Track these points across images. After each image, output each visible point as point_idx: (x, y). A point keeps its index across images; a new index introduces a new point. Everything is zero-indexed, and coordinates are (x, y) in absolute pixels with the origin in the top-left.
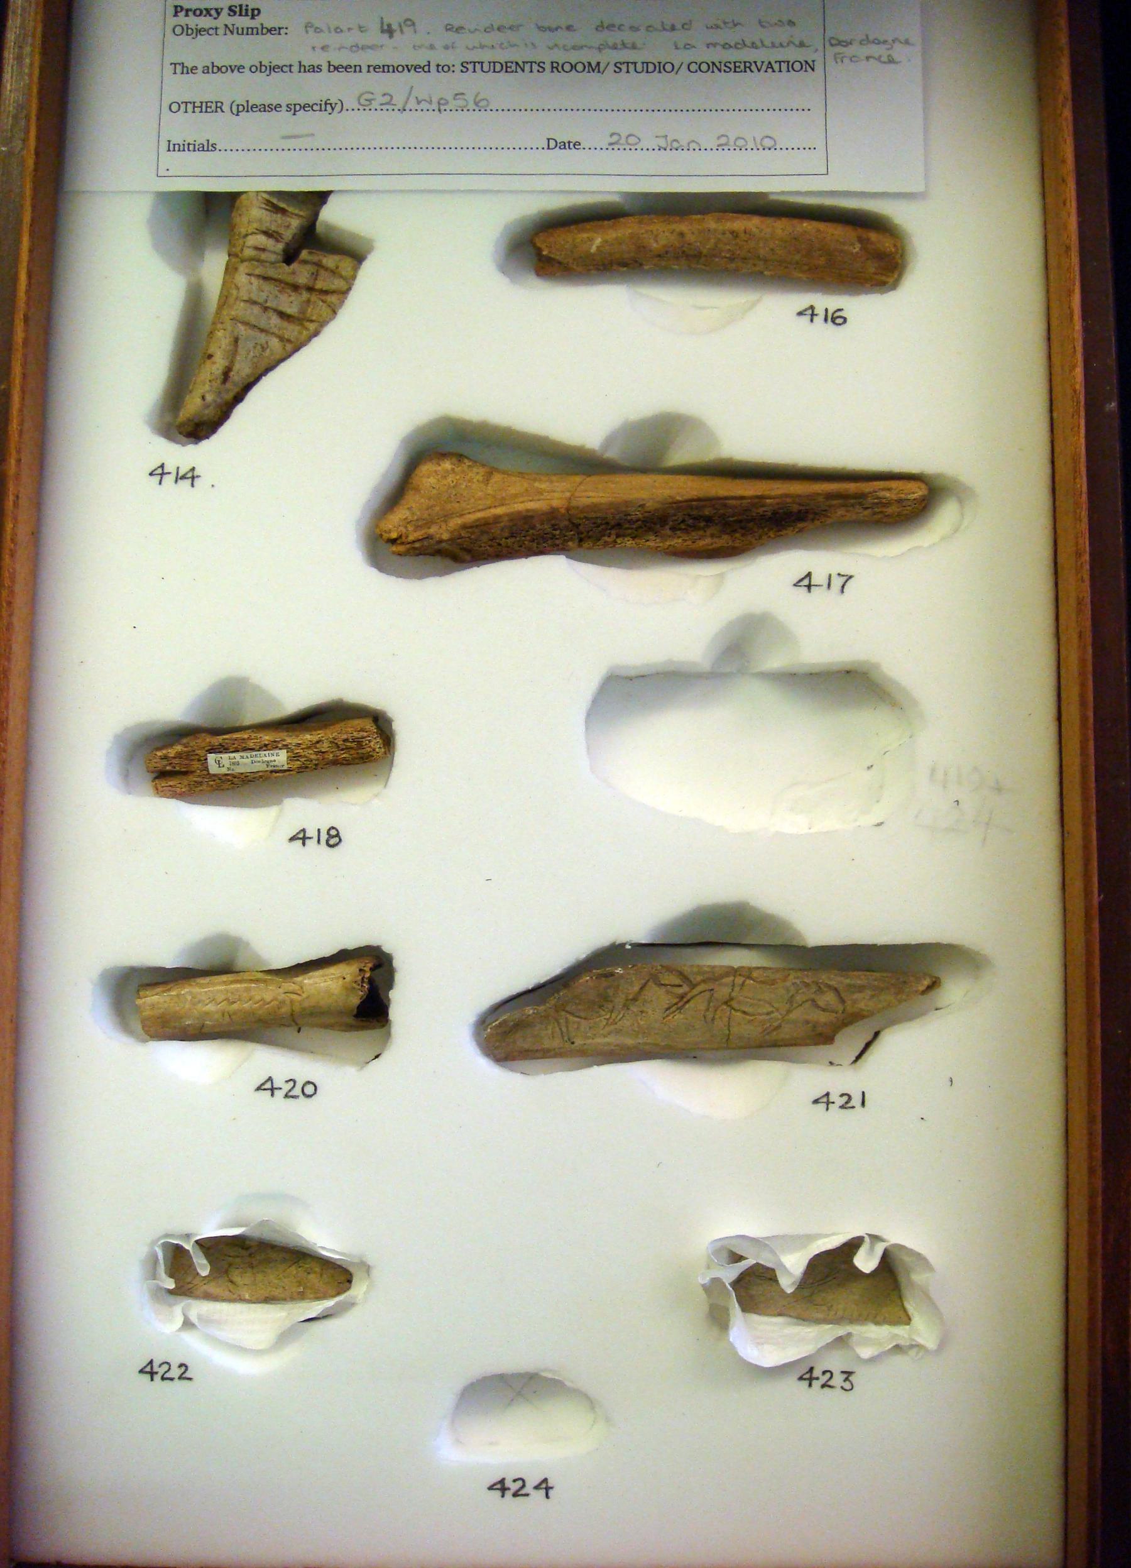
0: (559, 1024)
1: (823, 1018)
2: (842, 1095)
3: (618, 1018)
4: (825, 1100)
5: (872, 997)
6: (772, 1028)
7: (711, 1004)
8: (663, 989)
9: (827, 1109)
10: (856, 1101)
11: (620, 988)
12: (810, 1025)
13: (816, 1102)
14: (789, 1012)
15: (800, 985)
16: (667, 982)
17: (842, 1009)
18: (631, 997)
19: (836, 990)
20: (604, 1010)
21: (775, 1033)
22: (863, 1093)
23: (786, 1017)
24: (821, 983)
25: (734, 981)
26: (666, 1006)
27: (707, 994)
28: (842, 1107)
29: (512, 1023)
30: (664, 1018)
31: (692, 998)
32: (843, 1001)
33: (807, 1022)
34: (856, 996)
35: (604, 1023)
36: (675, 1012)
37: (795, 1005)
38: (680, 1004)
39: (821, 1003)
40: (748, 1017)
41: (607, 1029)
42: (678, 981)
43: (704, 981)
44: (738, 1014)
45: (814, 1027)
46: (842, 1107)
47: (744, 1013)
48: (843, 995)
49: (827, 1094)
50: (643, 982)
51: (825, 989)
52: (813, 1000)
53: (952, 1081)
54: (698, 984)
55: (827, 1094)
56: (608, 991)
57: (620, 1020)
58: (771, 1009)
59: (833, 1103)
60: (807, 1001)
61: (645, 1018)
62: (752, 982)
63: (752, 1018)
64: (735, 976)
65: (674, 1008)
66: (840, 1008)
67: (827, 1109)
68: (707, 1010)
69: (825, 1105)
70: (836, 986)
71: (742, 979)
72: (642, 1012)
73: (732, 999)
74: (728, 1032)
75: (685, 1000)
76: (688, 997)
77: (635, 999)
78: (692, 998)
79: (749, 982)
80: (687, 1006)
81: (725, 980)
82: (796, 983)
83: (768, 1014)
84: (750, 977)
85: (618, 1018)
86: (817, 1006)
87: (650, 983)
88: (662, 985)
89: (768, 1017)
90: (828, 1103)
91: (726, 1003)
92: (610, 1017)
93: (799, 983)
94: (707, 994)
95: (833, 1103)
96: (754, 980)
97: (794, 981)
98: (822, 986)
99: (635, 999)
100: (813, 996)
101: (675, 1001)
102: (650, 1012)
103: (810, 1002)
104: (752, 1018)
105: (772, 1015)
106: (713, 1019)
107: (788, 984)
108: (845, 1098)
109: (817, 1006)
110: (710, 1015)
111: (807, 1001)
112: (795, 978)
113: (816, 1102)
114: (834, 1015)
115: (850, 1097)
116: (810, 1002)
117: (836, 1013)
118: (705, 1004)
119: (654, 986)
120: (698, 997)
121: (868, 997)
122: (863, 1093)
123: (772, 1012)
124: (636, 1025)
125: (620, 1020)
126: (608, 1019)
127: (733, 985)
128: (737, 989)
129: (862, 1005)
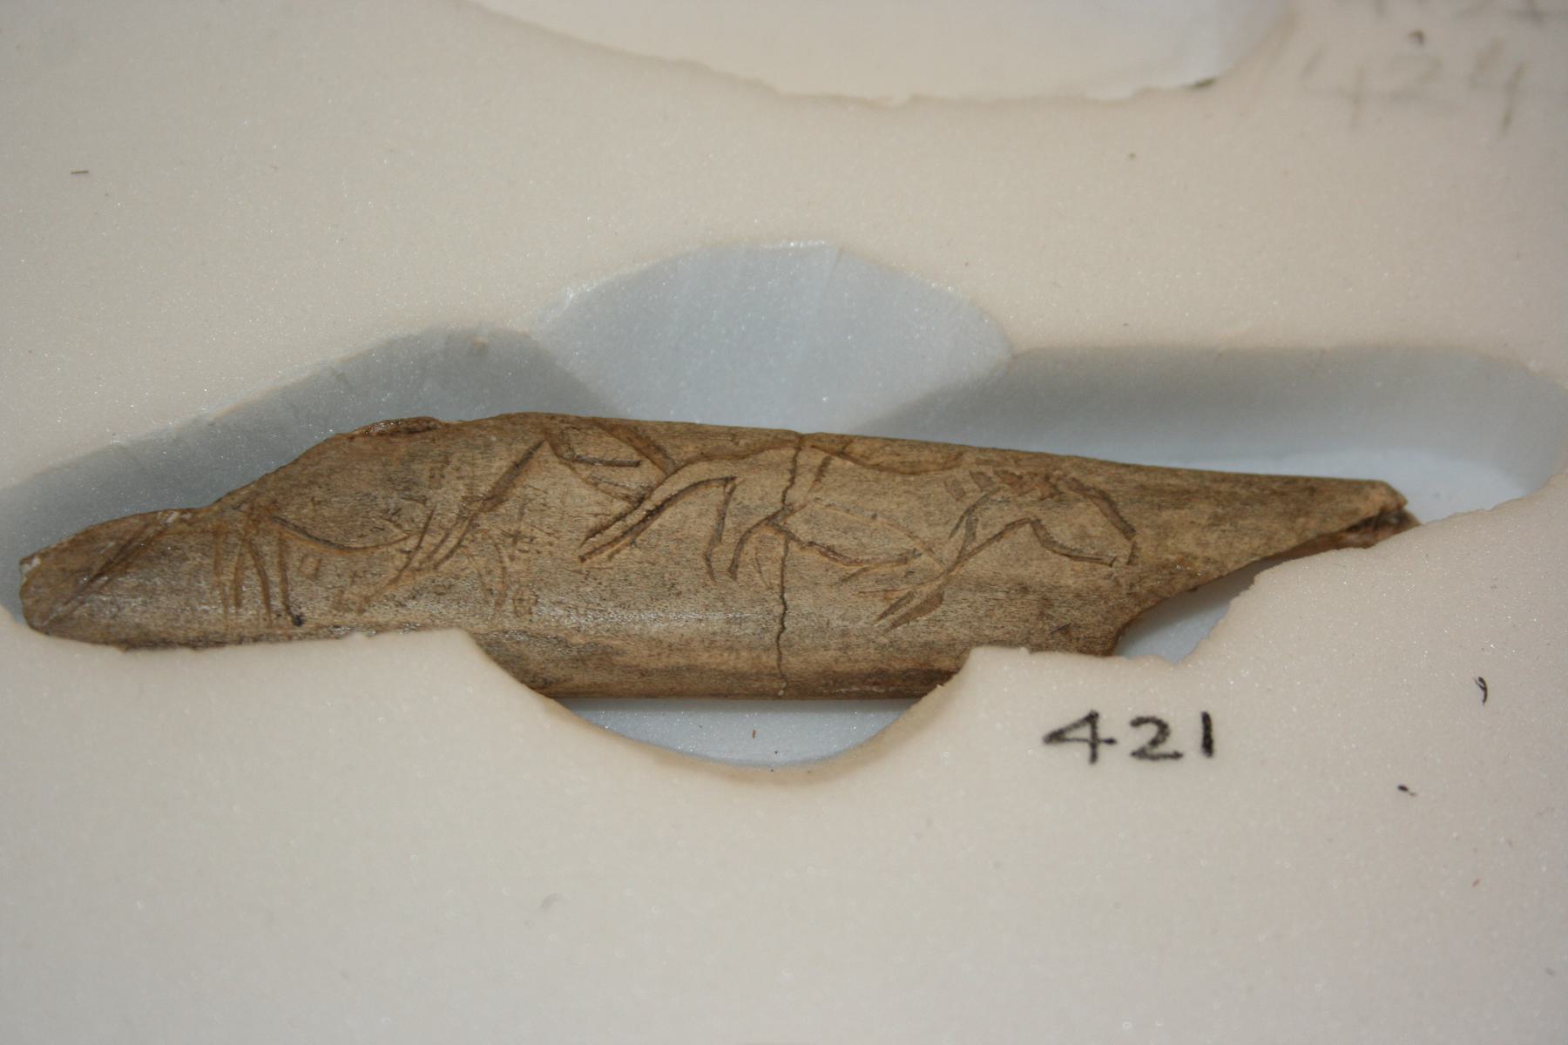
0: (257, 555)
1: (1071, 577)
2: (1138, 722)
3: (443, 551)
4: (1085, 732)
5: (1216, 520)
6: (915, 602)
7: (729, 523)
8: (585, 472)
9: (1094, 757)
10: (1185, 736)
11: (454, 461)
12: (1031, 597)
13: (1056, 737)
14: (962, 557)
15: (996, 479)
16: (594, 453)
17: (1127, 552)
18: (483, 489)
19: (1104, 496)
20: (399, 526)
21: (923, 619)
22: (1206, 719)
23: (960, 571)
24: (1059, 478)
25: (794, 460)
26: (592, 522)
27: (716, 494)
28: (1140, 754)
29: (111, 544)
30: (583, 559)
31: (669, 501)
32: (1128, 531)
33: (1025, 590)
34: (1166, 515)
35: (400, 560)
36: (616, 540)
37: (982, 534)
38: (632, 520)
39: (1062, 532)
40: (839, 566)
41: (407, 584)
42: (626, 453)
43: (707, 457)
44: (812, 556)
45: (1046, 602)
46: (1140, 754)
47: (829, 551)
48: (1126, 512)
49: (1092, 719)
50: (522, 447)
51: (1071, 494)
52: (1036, 524)
53: (1485, 689)
54: (689, 462)
55: (1092, 719)
56: (415, 466)
57: (447, 557)
58: (908, 544)
59: (1111, 741)
60: (1021, 523)
61: (524, 556)
62: (849, 463)
63: (855, 569)
64: (799, 449)
65: (614, 531)
66: (1121, 550)
67: (1094, 757)
68: (717, 537)
69: (1085, 749)
70: (1102, 487)
71: (818, 458)
72: (516, 537)
73: (787, 508)
74: (779, 610)
75: (648, 505)
76: (658, 497)
77: (495, 498)
78: (669, 501)
79: (837, 462)
80: (655, 525)
81: (772, 455)
82: (982, 474)
83: (904, 559)
84: (843, 454)
85: (443, 551)
86: (1048, 543)
87: (545, 451)
88: (579, 460)
89: (900, 570)
90: (1094, 743)
91: (770, 520)
92: (418, 547)
93: (990, 474)
94: (716, 494)
95: (1111, 741)
96: (855, 461)
97: (975, 469)
98: (1062, 487)
99: (495, 498)
100: (1036, 511)
101: (619, 506)
102: (540, 537)
103: (1028, 527)
104: (855, 569)
105: (916, 563)
106: (733, 570)
107: (959, 474)
108: (1150, 731)
109: (1048, 543)
110: (723, 557)
111: (1021, 523)
112: (979, 462)
113: (1056, 737)
114: (1105, 570)
115: (1163, 728)
116: (1028, 527)
117: (1111, 565)
118: (710, 521)
119: (553, 459)
120: (690, 498)
121: (1204, 521)
122: (1206, 719)
123: (915, 554)
124: (498, 572)
125: (447, 557)
126: (410, 554)
127: (794, 472)
128: (805, 479)
129: (1187, 542)
